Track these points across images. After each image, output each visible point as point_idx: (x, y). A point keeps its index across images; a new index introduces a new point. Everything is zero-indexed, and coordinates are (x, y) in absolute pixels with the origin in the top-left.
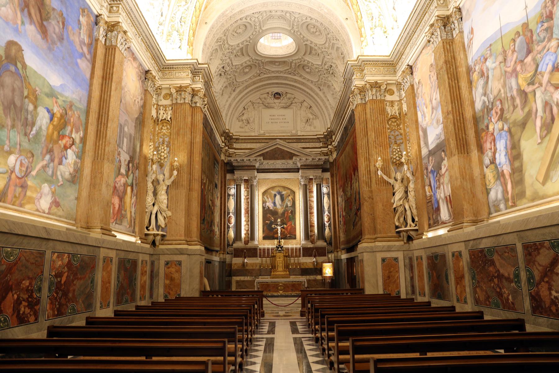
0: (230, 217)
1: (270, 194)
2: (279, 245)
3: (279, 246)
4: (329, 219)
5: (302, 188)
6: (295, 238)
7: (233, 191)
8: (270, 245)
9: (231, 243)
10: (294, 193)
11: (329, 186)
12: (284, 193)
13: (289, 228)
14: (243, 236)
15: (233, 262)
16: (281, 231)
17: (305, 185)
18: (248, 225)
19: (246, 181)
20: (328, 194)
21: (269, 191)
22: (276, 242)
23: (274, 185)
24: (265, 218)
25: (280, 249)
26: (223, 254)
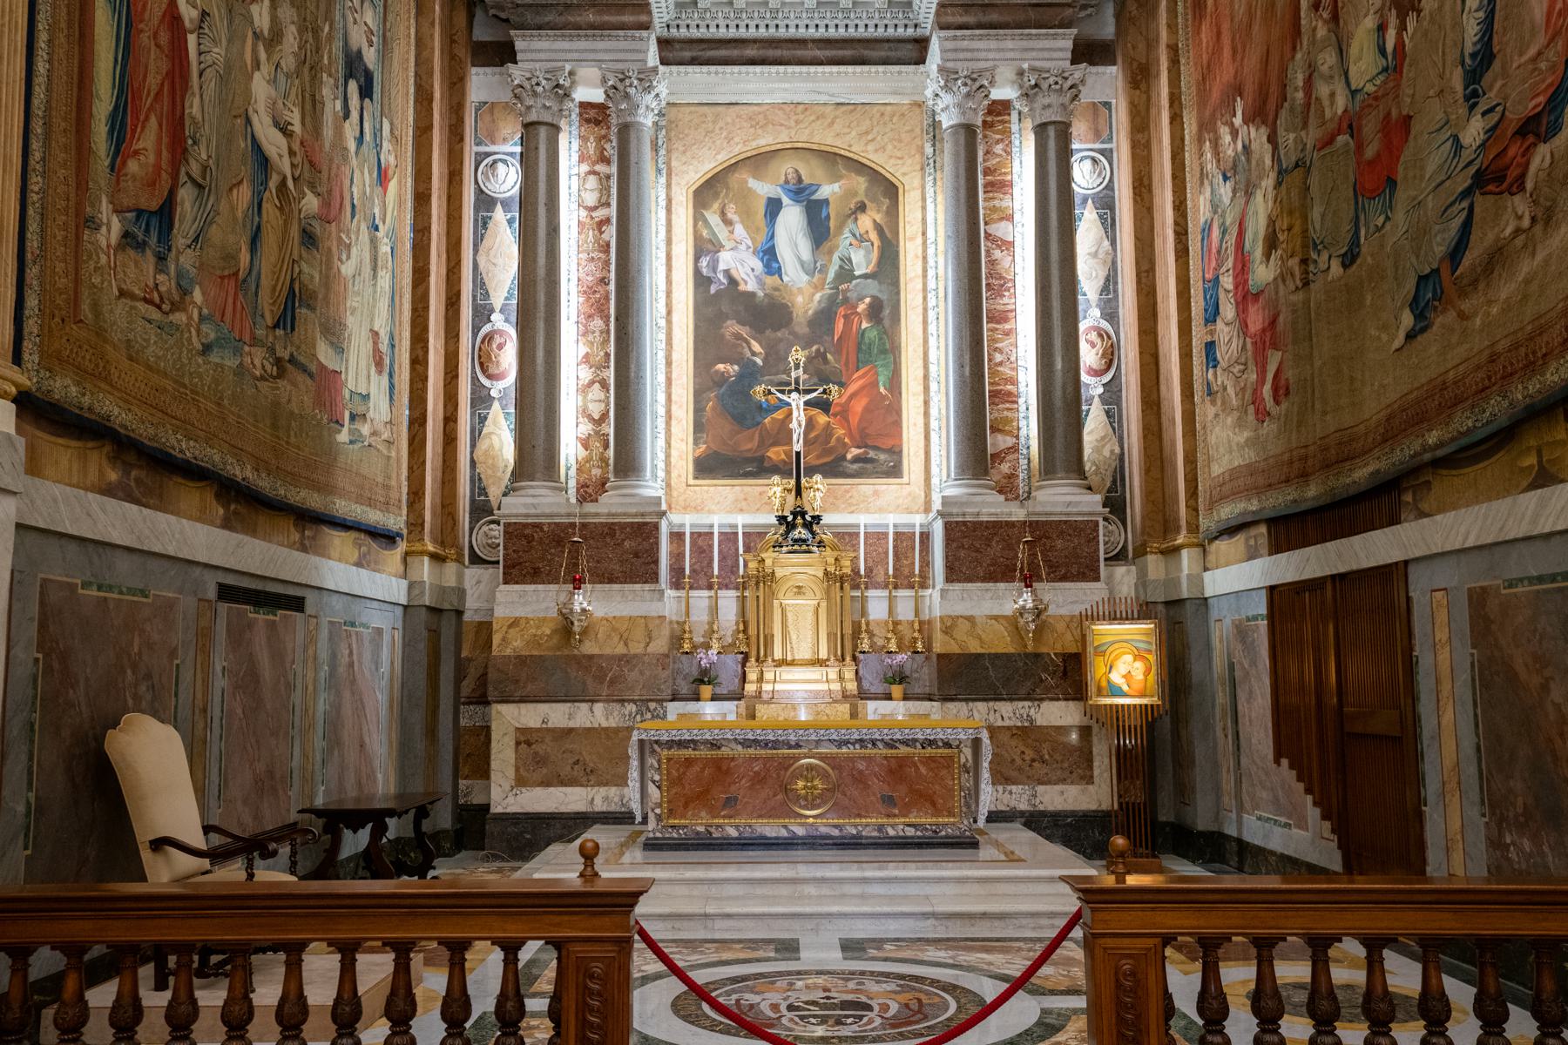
0: (489, 338)
1: (745, 196)
2: (799, 512)
3: (798, 525)
4: (1110, 356)
5: (947, 158)
6: (895, 471)
7: (507, 180)
8: (737, 508)
9: (494, 492)
10: (889, 190)
11: (1108, 154)
12: (827, 190)
13: (859, 406)
14: (570, 449)
15: (499, 612)
16: (810, 423)
17: (968, 130)
18: (604, 385)
19: (594, 115)
20: (1106, 203)
21: (735, 179)
22: (776, 489)
23: (765, 141)
24: (709, 343)
25: (800, 533)
26: (436, 558)
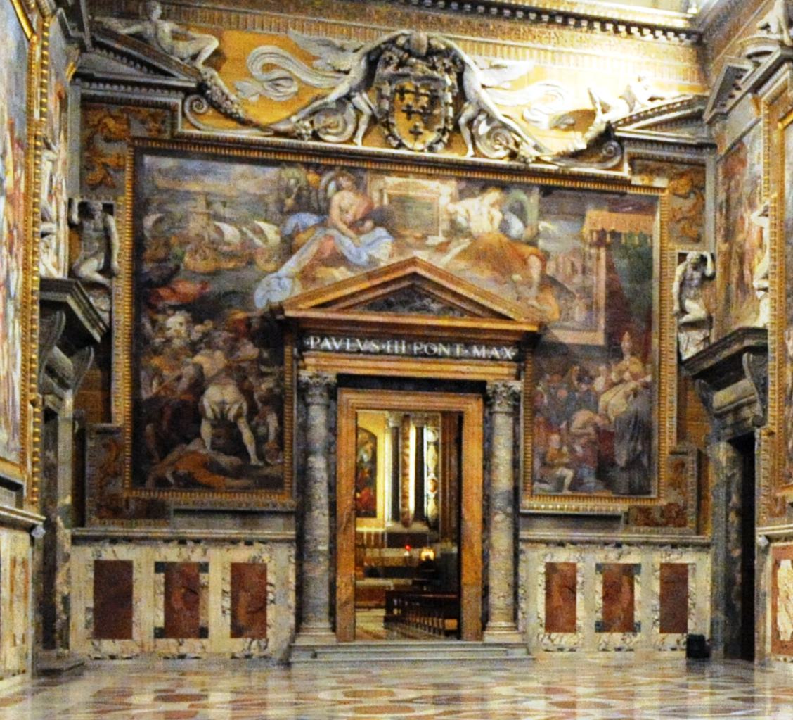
4: (436, 488)
10: (374, 438)
13: (366, 498)
20: (436, 444)
